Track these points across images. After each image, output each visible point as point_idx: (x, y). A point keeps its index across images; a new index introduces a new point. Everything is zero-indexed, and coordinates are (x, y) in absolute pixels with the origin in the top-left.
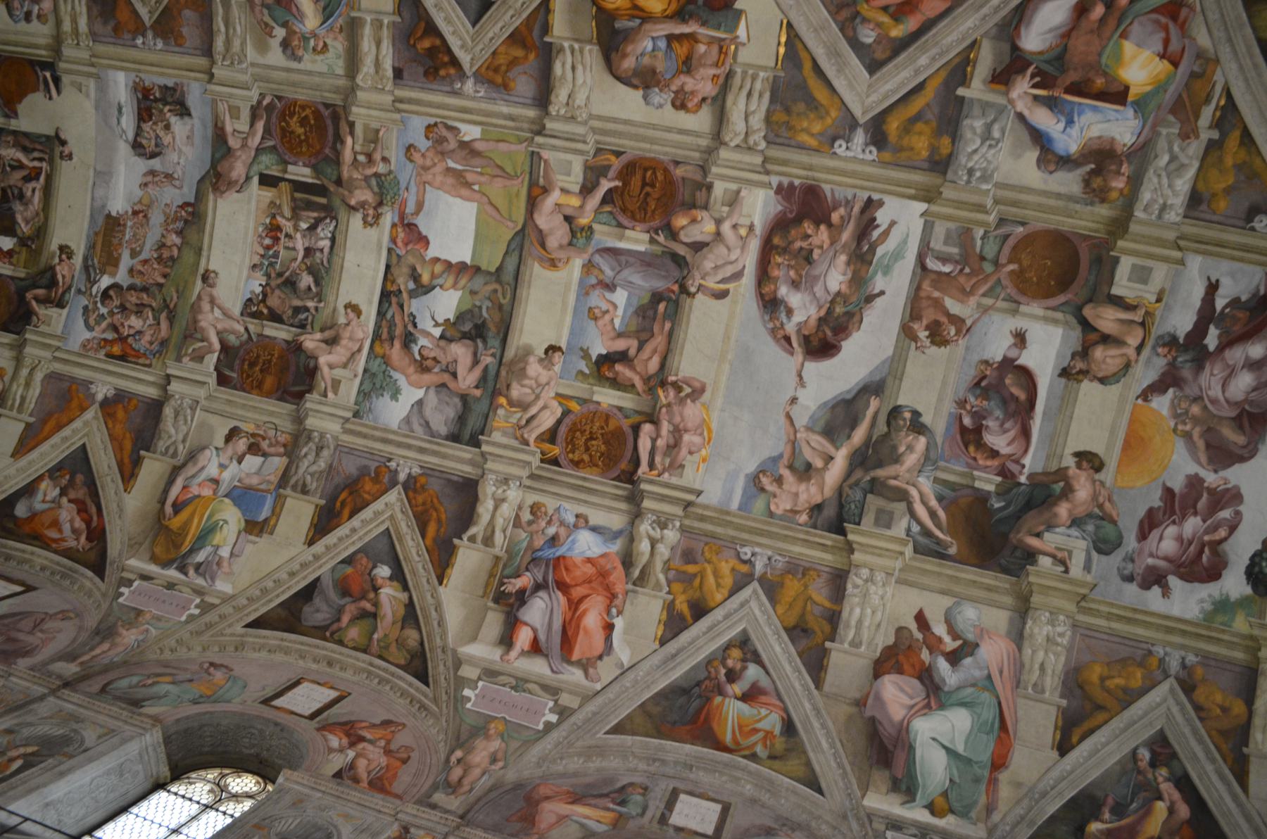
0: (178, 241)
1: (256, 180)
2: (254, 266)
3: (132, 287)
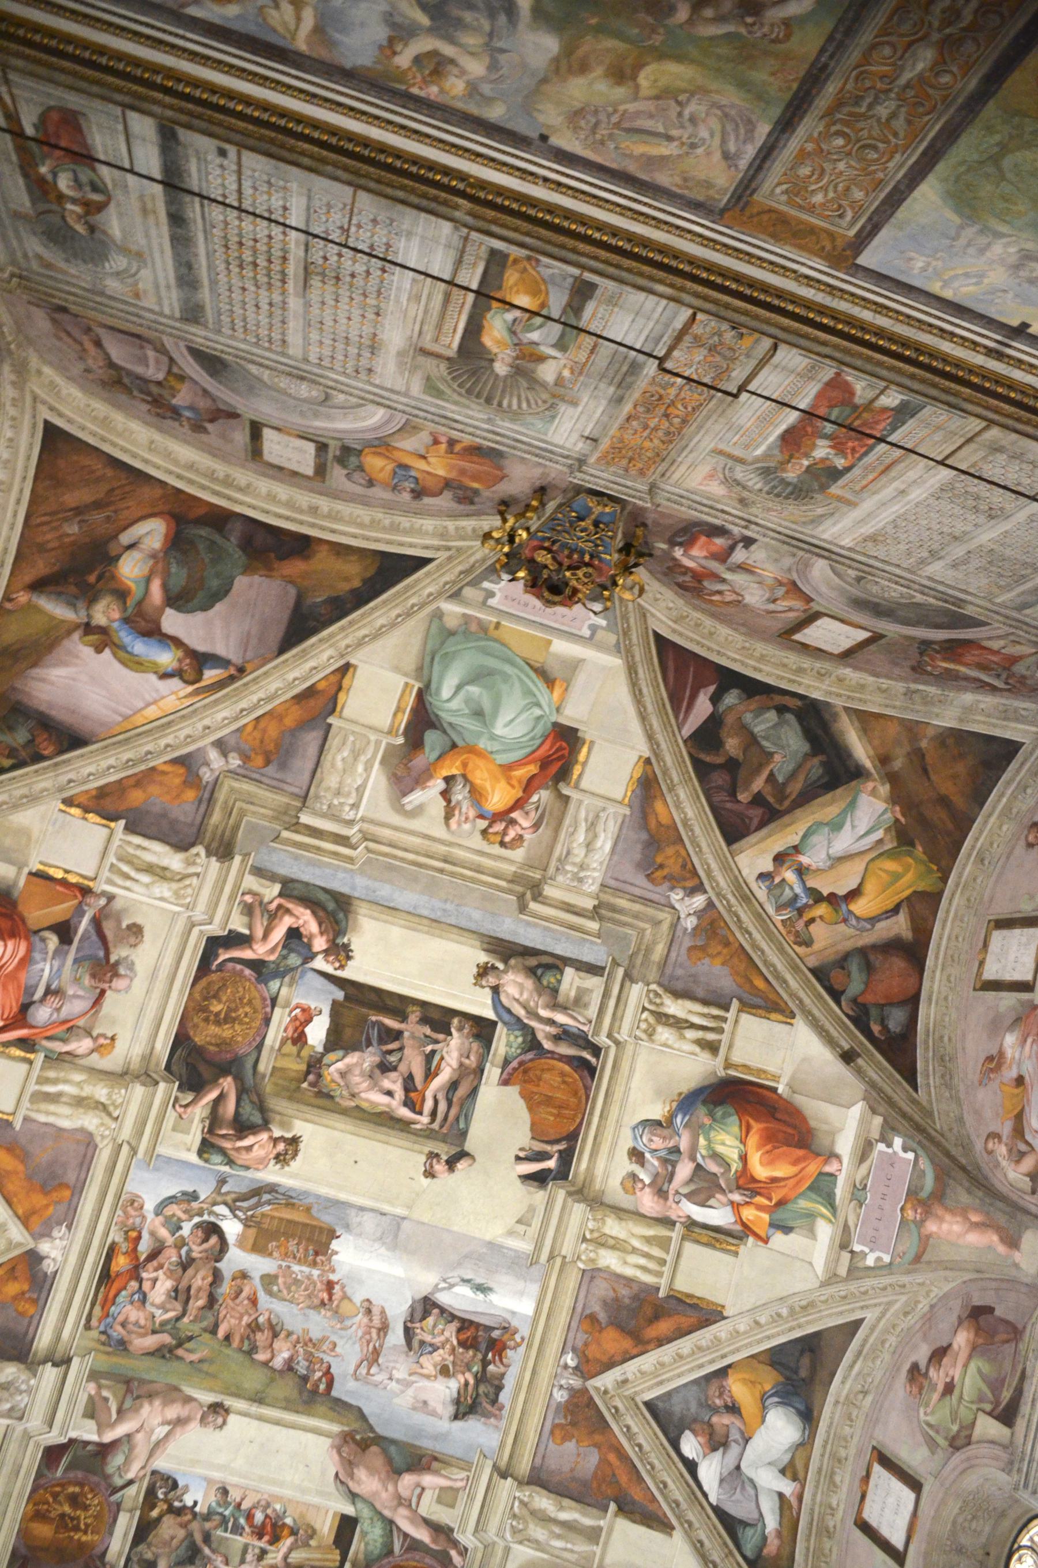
0: (278, 1362)
1: (350, 1510)
2: (225, 1492)
3: (217, 1276)
